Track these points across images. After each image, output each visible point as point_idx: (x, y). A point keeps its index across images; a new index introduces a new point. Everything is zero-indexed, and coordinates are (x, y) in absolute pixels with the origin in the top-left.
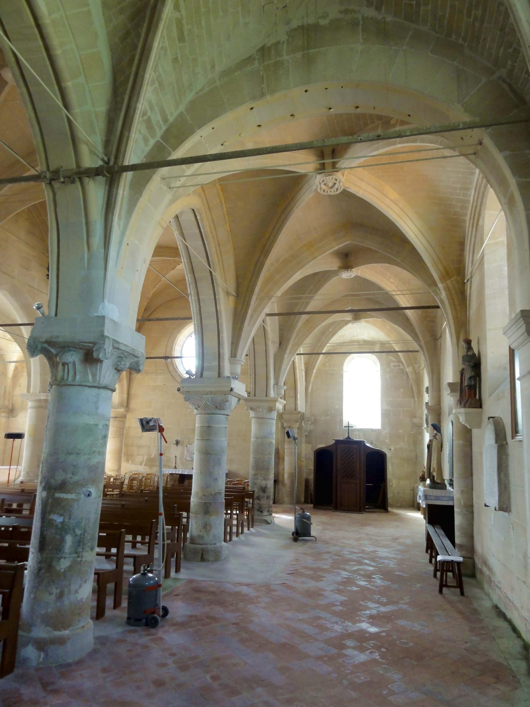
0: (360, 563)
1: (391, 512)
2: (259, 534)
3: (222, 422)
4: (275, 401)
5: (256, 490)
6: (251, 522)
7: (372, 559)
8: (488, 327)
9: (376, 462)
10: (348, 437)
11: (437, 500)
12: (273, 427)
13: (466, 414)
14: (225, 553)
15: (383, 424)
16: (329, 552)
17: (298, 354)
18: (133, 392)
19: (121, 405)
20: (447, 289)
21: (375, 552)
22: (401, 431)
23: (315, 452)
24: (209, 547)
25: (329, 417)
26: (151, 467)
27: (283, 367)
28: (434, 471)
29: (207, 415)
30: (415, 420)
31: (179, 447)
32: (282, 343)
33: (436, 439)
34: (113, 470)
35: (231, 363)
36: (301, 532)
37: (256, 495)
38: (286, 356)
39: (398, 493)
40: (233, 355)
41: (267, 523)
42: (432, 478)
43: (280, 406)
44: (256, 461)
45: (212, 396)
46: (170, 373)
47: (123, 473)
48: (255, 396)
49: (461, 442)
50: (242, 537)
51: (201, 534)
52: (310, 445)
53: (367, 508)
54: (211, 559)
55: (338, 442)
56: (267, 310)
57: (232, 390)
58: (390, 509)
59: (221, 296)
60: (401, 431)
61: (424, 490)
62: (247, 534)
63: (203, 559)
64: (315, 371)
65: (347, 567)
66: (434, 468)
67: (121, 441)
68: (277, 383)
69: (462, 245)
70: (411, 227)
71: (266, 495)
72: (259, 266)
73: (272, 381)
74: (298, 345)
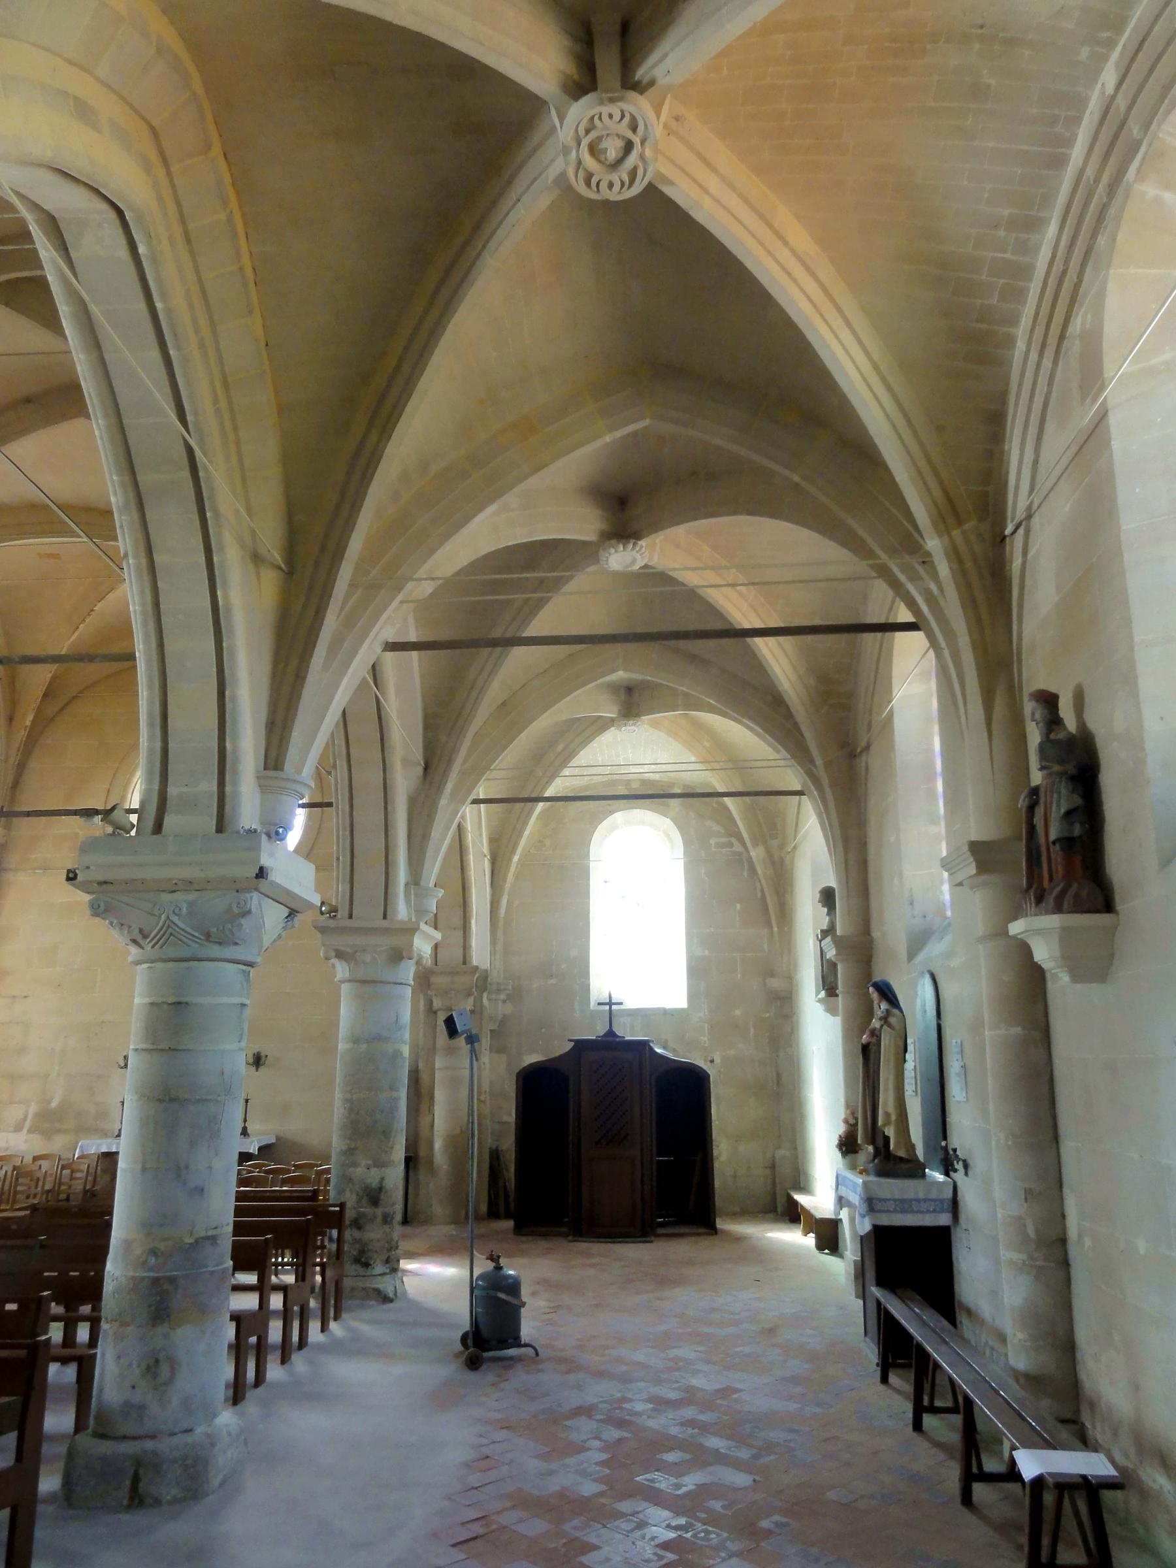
0: (701, 1458)
1: (724, 1232)
2: (357, 1348)
3: (225, 987)
4: (410, 930)
5: (350, 1199)
6: (334, 1302)
7: (742, 1440)
8: (1139, 636)
9: (679, 1098)
10: (611, 1033)
11: (903, 1211)
12: (405, 1007)
13: (1066, 934)
14: (223, 1459)
15: (692, 996)
16: (585, 1411)
17: (476, 801)
20: (954, 555)
21: (726, 1392)
22: (737, 1012)
23: (518, 1075)
24: (164, 1446)
25: (553, 981)
26: (47, 1134)
27: (435, 834)
28: (887, 1123)
29: (171, 965)
30: (775, 983)
32: (433, 764)
33: (890, 1026)
35: (264, 785)
36: (491, 1335)
37: (350, 1214)
38: (443, 802)
39: (735, 1177)
40: (274, 759)
41: (386, 1299)
42: (880, 1143)
43: (422, 946)
44: (351, 1111)
45: (192, 896)
48: (351, 917)
49: (1018, 1030)
50: (298, 1360)
51: (137, 1398)
52: (504, 1058)
53: (661, 1225)
54: (168, 1492)
55: (581, 1046)
56: (388, 629)
57: (262, 873)
58: (721, 1224)
59: (231, 557)
60: (737, 1012)
61: (864, 1183)
62: (321, 1348)
63: (137, 1499)
64: (516, 858)
65: (663, 1482)
66: (887, 1115)
68: (415, 879)
69: (994, 422)
70: (852, 354)
71: (379, 1211)
72: (363, 464)
73: (402, 875)
74: (477, 772)
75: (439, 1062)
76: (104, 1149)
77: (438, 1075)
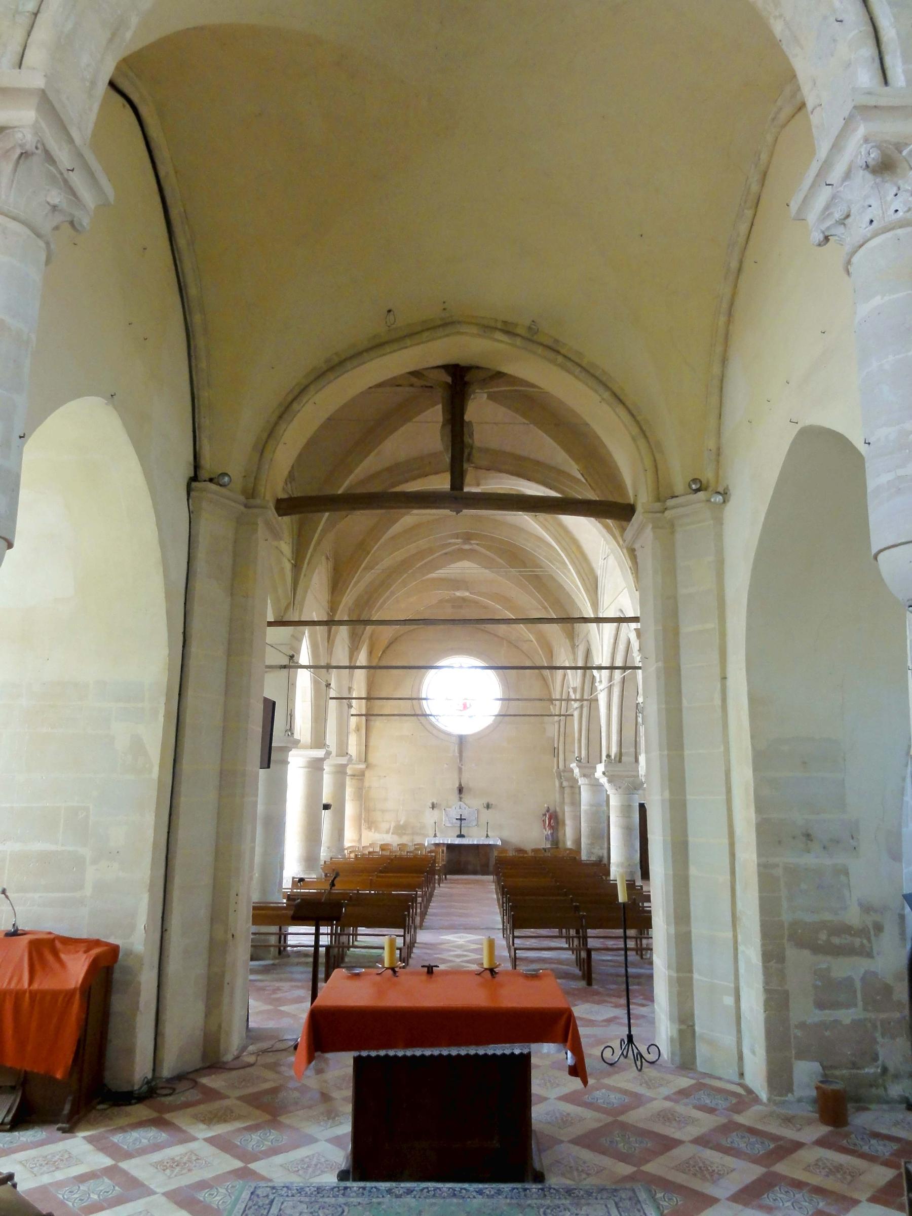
18: (372, 742)
26: (400, 835)
31: (436, 811)
34: (354, 841)
47: (365, 842)
67: (361, 806)
77: (566, 814)
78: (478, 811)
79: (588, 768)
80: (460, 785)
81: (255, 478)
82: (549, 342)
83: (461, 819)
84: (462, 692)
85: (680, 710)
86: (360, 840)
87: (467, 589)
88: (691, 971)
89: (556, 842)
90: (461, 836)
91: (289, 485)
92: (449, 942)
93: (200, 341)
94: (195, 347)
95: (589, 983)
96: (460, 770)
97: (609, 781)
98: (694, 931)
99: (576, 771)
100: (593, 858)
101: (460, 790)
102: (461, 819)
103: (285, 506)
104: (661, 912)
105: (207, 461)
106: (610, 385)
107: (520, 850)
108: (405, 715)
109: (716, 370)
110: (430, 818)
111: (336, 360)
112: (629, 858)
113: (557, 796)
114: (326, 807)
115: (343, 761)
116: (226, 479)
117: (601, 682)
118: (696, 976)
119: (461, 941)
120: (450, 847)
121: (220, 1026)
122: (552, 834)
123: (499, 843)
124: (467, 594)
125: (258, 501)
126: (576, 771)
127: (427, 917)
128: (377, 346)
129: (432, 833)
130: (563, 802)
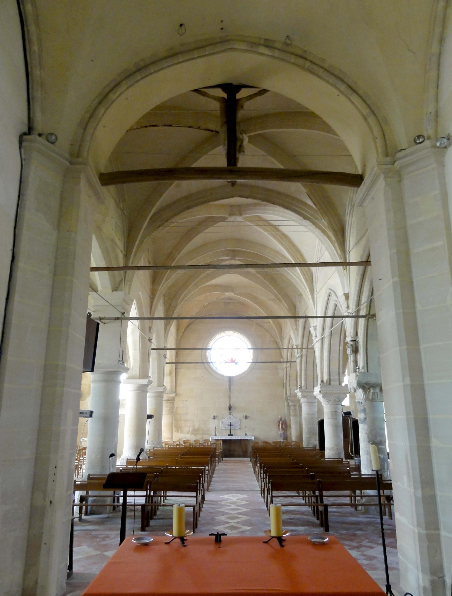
18: (179, 382)
19: (171, 392)
23: (318, 422)
26: (195, 435)
31: (216, 420)
46: (206, 368)
47: (175, 439)
67: (172, 417)
75: (292, 418)
76: (217, 438)
77: (292, 422)
78: (240, 420)
79: (307, 391)
80: (230, 405)
81: (80, 146)
82: (300, 53)
83: (230, 425)
84: (230, 352)
85: (415, 314)
86: (172, 438)
87: (233, 292)
88: (438, 529)
89: (286, 438)
90: (230, 435)
91: (122, 204)
92: (227, 499)
93: (32, 28)
94: (28, 31)
95: (327, 530)
96: (230, 397)
97: (324, 397)
98: (439, 494)
99: (299, 394)
100: (311, 446)
101: (230, 408)
102: (230, 425)
103: (107, 179)
104: (405, 478)
105: (39, 125)
106: (346, 80)
107: (266, 443)
108: (198, 363)
109: (435, 49)
110: (213, 424)
111: (142, 64)
112: (337, 445)
113: (286, 411)
114: (150, 417)
115: (161, 389)
116: (53, 137)
117: (316, 336)
118: (443, 533)
119: (234, 499)
120: (225, 441)
121: (36, 583)
122: (284, 433)
123: (253, 438)
124: (233, 294)
125: (80, 160)
126: (299, 394)
127: (212, 483)
128: (172, 55)
129: (213, 433)
130: (289, 415)
